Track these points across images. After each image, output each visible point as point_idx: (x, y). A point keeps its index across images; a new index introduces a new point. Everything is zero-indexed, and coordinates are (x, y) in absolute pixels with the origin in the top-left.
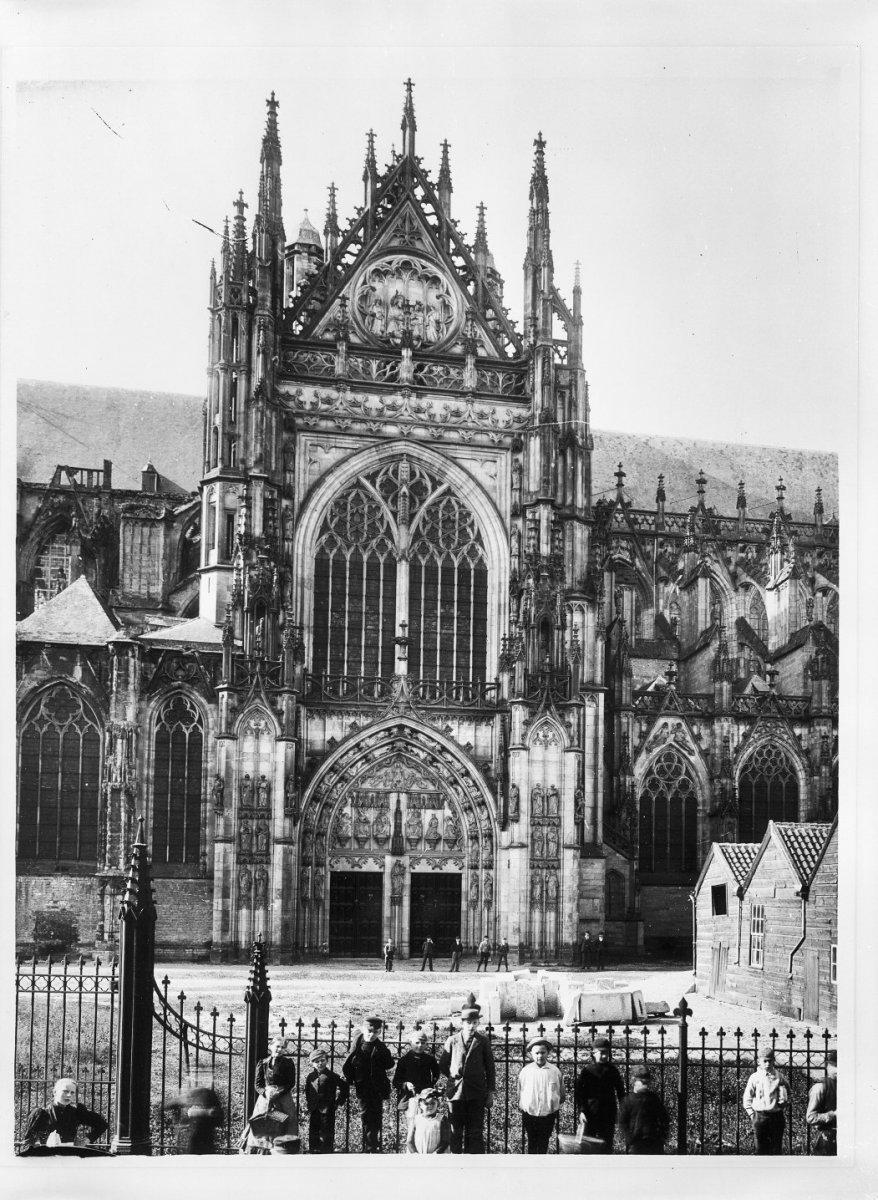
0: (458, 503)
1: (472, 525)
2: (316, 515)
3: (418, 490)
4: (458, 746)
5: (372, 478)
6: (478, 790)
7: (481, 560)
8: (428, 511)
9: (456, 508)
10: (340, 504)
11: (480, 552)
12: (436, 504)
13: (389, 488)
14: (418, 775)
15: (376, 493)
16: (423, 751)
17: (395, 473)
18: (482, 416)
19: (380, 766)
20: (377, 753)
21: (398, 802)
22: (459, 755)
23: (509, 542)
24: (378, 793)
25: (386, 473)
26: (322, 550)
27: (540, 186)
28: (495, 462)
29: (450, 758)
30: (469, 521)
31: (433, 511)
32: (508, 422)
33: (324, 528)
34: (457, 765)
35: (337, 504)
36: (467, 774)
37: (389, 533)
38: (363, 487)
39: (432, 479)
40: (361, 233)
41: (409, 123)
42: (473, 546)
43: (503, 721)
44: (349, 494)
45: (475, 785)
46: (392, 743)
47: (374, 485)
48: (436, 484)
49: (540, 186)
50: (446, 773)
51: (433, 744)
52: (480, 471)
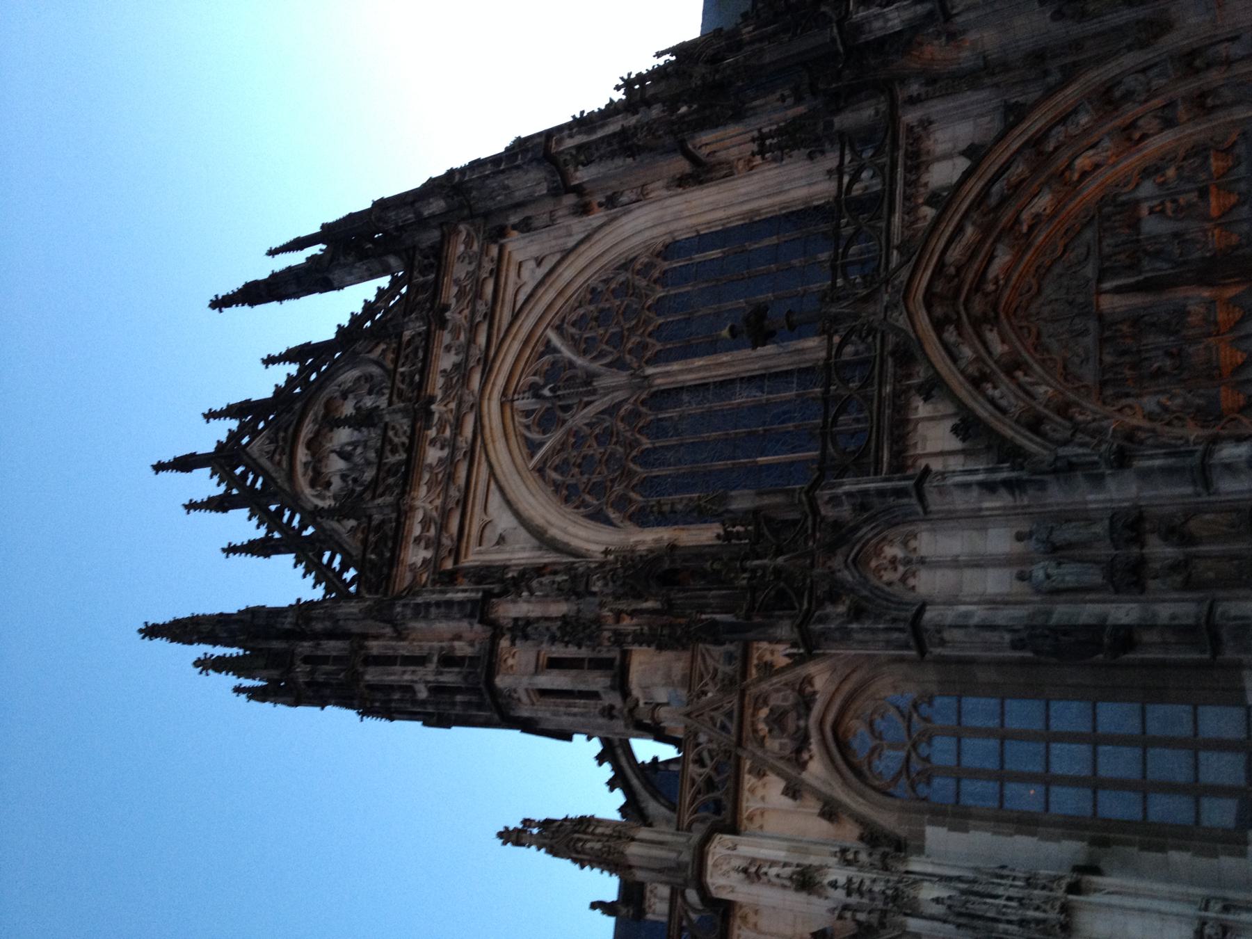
0: (574, 309)
1: (606, 281)
2: (572, 529)
3: (557, 372)
4: (967, 175)
5: (533, 447)
6: (1075, 112)
7: (659, 255)
8: (585, 353)
9: (581, 311)
10: (567, 495)
11: (644, 260)
12: (574, 343)
13: (546, 422)
14: (1057, 270)
15: (552, 439)
16: (991, 258)
17: (527, 414)
18: (460, 295)
19: (1039, 346)
20: (999, 348)
21: (1118, 290)
22: (991, 167)
23: (627, 208)
24: (1102, 341)
25: (528, 427)
26: (631, 518)
27: (253, 294)
28: (520, 265)
29: (996, 188)
30: (601, 287)
31: (583, 346)
32: (470, 257)
33: (598, 517)
34: (1019, 169)
35: (566, 500)
36: (1036, 142)
37: (612, 410)
38: (544, 461)
39: (542, 355)
40: (273, 508)
41: (186, 463)
42: (638, 272)
43: (913, 101)
44: (554, 483)
45: (1063, 120)
46: (977, 323)
47: (541, 444)
48: (549, 348)
49: (253, 294)
50: (1044, 202)
51: (969, 230)
52: (530, 275)
